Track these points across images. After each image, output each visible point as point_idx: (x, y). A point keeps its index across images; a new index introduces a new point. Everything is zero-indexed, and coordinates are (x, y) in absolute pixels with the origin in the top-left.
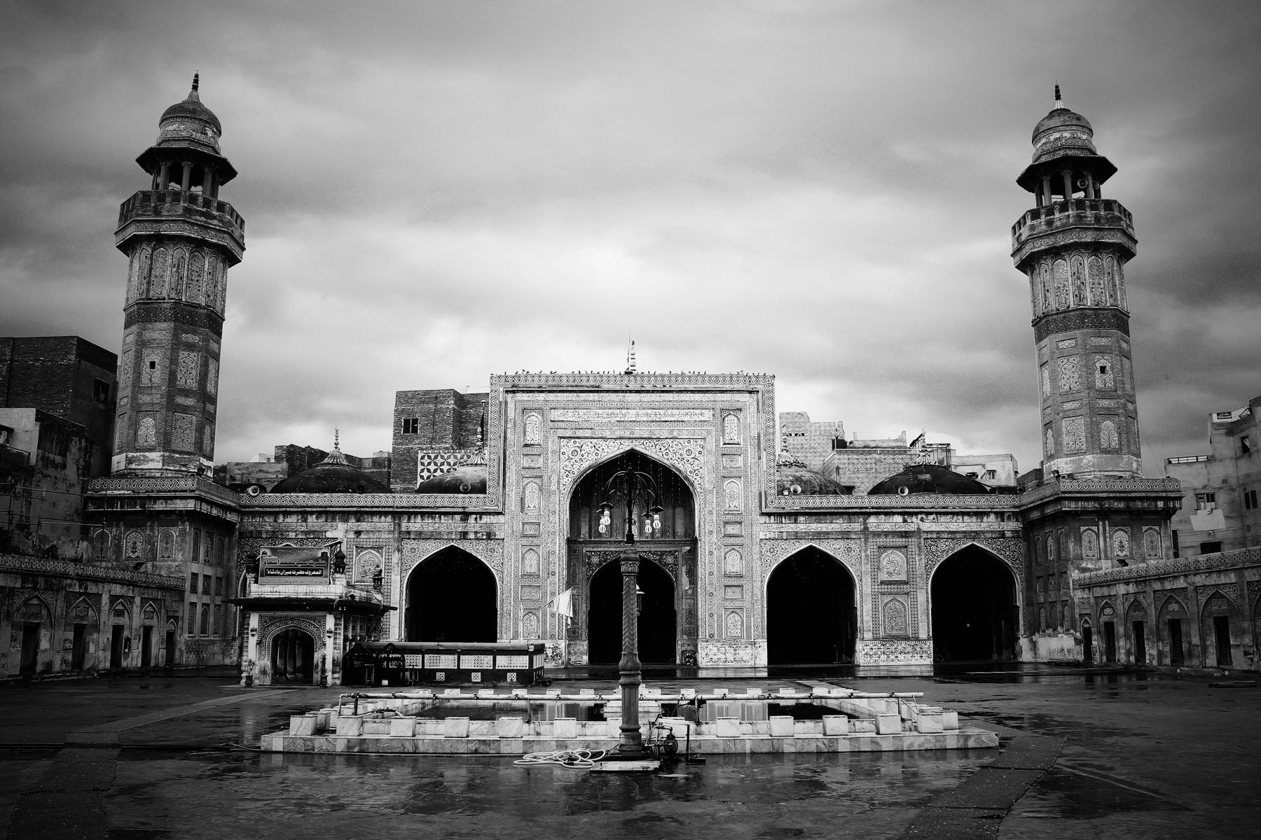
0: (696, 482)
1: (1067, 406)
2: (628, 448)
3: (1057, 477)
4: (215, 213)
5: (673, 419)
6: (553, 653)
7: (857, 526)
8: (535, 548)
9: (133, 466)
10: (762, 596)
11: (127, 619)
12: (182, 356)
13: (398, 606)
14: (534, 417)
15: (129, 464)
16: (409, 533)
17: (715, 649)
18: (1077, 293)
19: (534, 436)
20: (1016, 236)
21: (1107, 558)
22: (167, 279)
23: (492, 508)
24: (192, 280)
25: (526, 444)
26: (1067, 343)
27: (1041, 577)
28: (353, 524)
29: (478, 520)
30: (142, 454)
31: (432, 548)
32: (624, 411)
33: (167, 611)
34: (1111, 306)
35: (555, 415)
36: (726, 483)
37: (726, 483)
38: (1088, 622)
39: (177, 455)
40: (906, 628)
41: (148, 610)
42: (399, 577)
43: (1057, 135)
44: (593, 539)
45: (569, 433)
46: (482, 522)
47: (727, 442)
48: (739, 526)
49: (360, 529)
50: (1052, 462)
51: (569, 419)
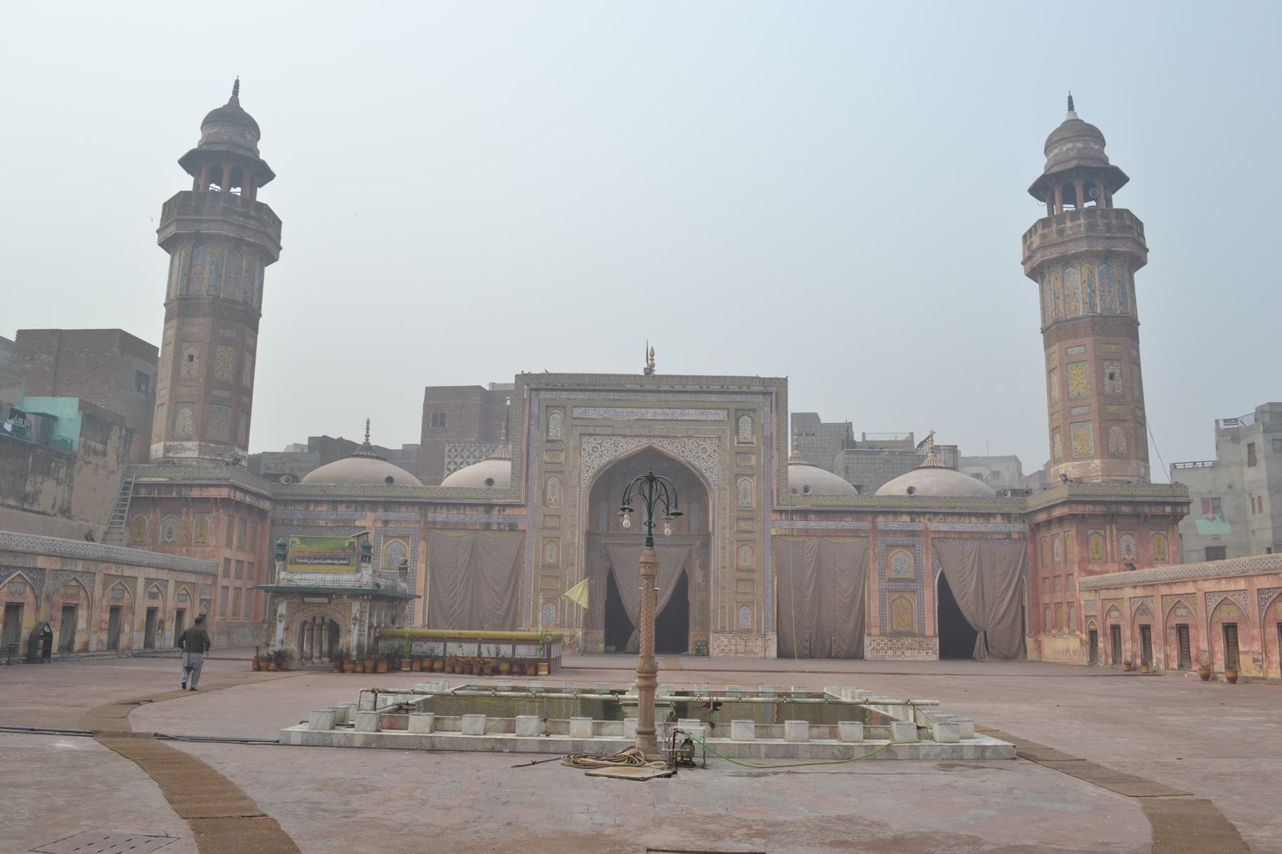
0: (710, 480)
1: (1075, 411)
3: (1064, 481)
4: (253, 213)
7: (866, 524)
8: (555, 540)
9: (171, 455)
10: (773, 590)
11: (162, 602)
12: (219, 350)
13: (421, 594)
14: (556, 415)
15: (167, 452)
16: (435, 523)
17: (726, 641)
18: (1087, 301)
19: (556, 431)
21: (1113, 561)
22: (206, 276)
23: (516, 501)
24: (230, 277)
25: (549, 441)
26: (1077, 349)
27: (1047, 578)
28: (381, 513)
29: (501, 512)
30: (179, 443)
32: (643, 410)
33: (200, 595)
34: (1121, 313)
35: (578, 412)
37: (740, 480)
38: (1094, 625)
39: (212, 445)
40: (912, 624)
41: (181, 593)
43: (1070, 145)
44: (611, 532)
45: (591, 431)
46: (505, 514)
48: (751, 522)
49: (388, 518)
50: (1060, 466)
51: (590, 417)
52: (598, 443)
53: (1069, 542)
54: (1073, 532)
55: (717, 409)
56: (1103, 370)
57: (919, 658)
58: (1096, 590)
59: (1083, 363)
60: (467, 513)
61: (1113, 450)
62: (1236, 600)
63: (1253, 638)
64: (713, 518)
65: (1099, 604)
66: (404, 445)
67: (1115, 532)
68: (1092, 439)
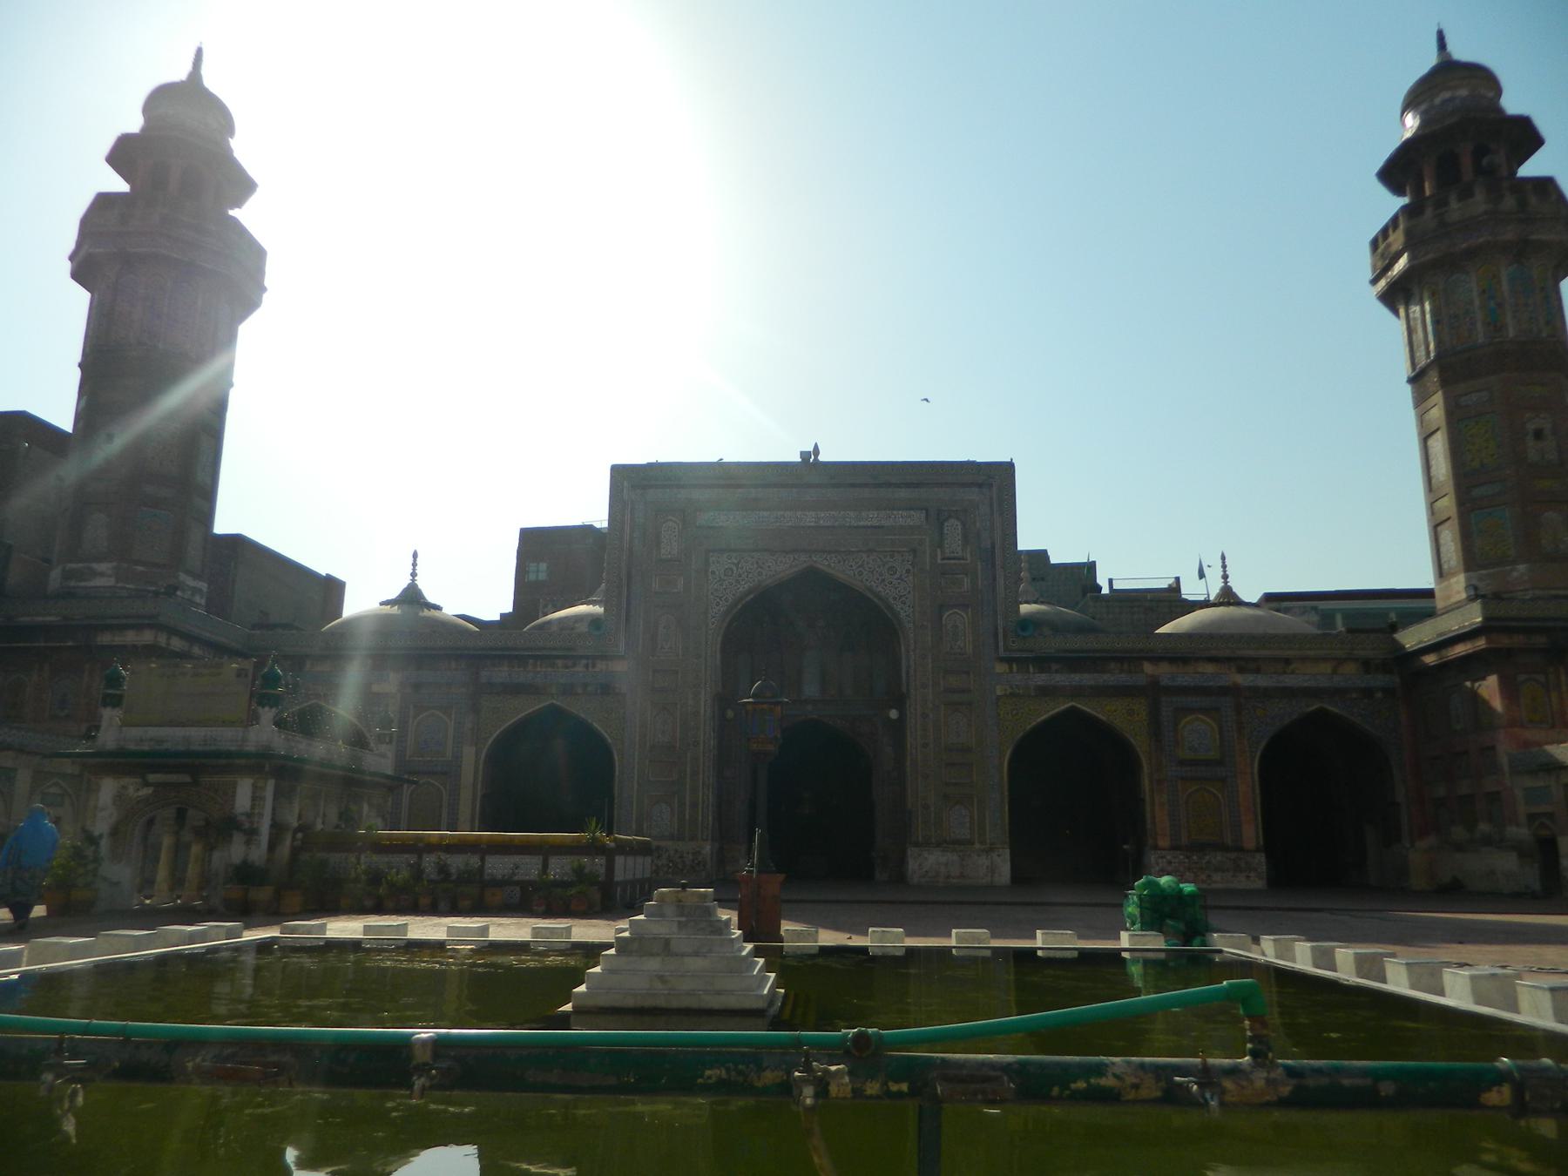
0: (903, 615)
1: (1476, 492)
2: (805, 565)
5: (869, 524)
6: (693, 861)
9: (72, 583)
14: (670, 524)
20: (1380, 250)
29: (590, 665)
31: (526, 707)
32: (799, 513)
36: (948, 613)
37: (945, 616)
39: (140, 568)
41: (52, 790)
42: (473, 749)
43: (1447, 95)
46: (597, 670)
47: (948, 555)
52: (733, 563)
55: (911, 509)
60: (539, 669)
64: (908, 673)
66: (502, 615)
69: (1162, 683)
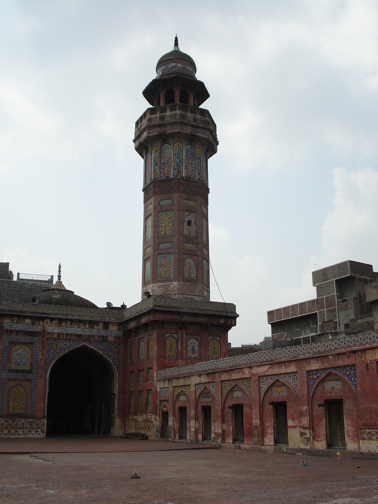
1: (162, 246)
18: (176, 167)
20: (138, 127)
26: (166, 202)
38: (166, 407)
43: (174, 64)
50: (148, 287)
53: (151, 343)
54: (155, 335)
56: (184, 218)
57: (30, 436)
58: (170, 380)
59: (170, 212)
61: (187, 276)
62: (286, 381)
63: (301, 414)
65: (171, 389)
67: (184, 336)
68: (173, 267)
69: (5, 328)
